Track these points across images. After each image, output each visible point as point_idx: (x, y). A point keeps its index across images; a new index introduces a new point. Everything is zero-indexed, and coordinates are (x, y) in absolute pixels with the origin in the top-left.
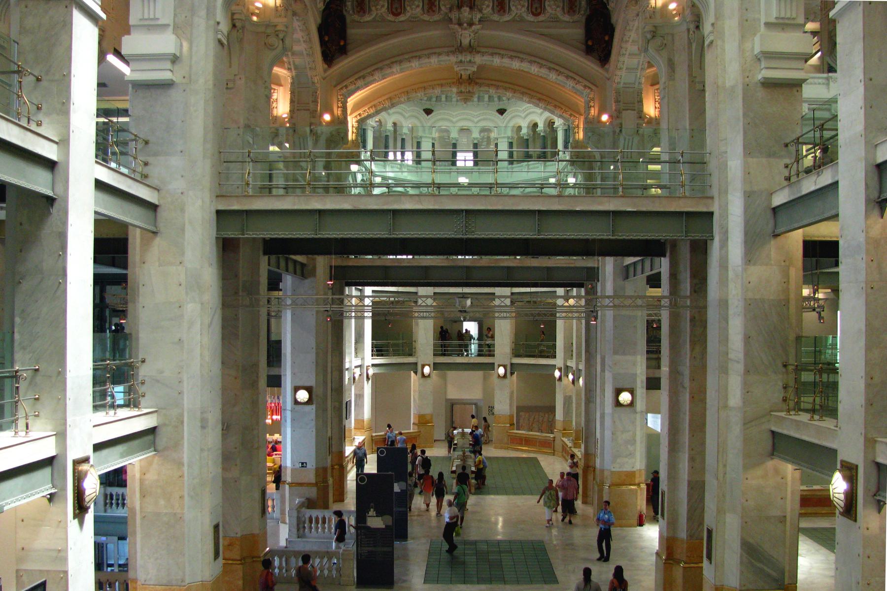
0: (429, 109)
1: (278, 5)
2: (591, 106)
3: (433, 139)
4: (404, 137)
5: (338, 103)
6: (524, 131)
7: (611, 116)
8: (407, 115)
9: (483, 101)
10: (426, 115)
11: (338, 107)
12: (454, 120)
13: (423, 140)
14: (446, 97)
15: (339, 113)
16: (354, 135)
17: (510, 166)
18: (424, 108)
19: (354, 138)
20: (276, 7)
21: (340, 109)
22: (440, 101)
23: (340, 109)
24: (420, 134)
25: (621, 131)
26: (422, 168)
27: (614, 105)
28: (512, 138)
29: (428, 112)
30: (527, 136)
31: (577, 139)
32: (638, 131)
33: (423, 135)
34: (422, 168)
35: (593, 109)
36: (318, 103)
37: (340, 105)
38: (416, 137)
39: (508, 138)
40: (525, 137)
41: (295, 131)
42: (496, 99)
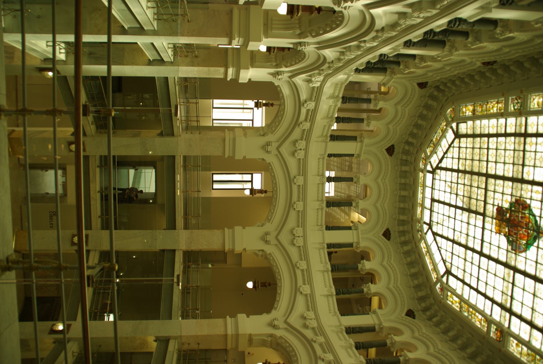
0: (393, 151)
3: (359, 156)
4: (365, 122)
6: (367, 265)
8: (391, 126)
9: (399, 213)
10: (386, 147)
12: (379, 180)
13: (359, 144)
14: (406, 172)
17: (326, 246)
18: (395, 147)
22: (401, 165)
24: (366, 141)
26: (326, 142)
28: (357, 248)
29: (390, 150)
30: (362, 269)
33: (364, 144)
34: (326, 142)
38: (361, 136)
39: (358, 243)
40: (360, 266)
42: (401, 228)
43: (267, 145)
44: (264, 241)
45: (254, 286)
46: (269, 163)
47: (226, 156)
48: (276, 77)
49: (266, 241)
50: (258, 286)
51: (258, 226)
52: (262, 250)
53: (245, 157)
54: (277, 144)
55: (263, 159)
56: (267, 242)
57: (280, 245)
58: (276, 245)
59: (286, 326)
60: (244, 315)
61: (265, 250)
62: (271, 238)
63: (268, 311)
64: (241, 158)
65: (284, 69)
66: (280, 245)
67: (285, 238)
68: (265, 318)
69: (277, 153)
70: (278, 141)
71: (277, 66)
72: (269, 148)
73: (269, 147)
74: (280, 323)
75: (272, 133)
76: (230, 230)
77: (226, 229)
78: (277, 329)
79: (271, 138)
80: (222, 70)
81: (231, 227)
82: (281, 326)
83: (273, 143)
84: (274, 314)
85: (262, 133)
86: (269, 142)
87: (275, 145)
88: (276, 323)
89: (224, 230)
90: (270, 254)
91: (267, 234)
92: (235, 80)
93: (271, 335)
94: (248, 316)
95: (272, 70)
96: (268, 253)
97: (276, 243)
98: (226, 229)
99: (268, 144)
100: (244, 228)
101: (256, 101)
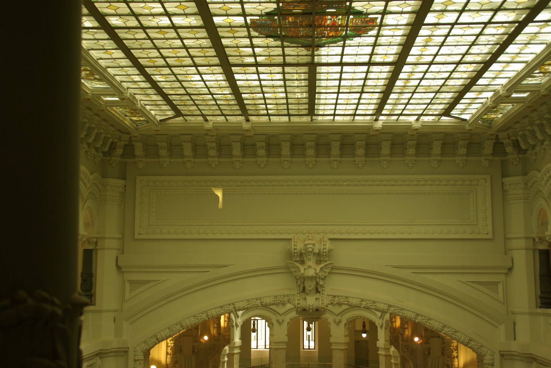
1: (168, 363)
2: (405, 328)
5: (214, 325)
7: (420, 337)
11: (214, 328)
15: (215, 332)
16: (226, 323)
19: (226, 325)
20: (167, 364)
21: (215, 329)
23: (215, 329)
25: (429, 353)
27: (423, 332)
31: (394, 327)
32: (442, 353)
35: (407, 330)
36: (199, 329)
37: (215, 326)
41: (181, 351)
43: (279, 321)
44: (339, 324)
45: (365, 333)
46: (290, 319)
47: (286, 347)
48: (238, 326)
49: (339, 322)
50: (364, 330)
51: (330, 326)
52: (345, 325)
53: (286, 335)
54: (278, 316)
55: (288, 323)
56: (340, 322)
57: (342, 313)
58: (341, 316)
59: (381, 319)
60: (378, 342)
61: (344, 323)
62: (338, 319)
63: (377, 327)
64: (287, 338)
65: (234, 323)
66: (342, 313)
67: (337, 310)
68: (379, 329)
69: (283, 315)
70: (276, 315)
71: (233, 326)
72: (281, 320)
73: (279, 321)
74: (381, 321)
75: (271, 320)
76: (333, 345)
77: (332, 347)
78: (383, 325)
79: (274, 321)
80: (235, 356)
81: (331, 344)
82: (381, 322)
83: (278, 318)
84: (377, 324)
85: (271, 325)
86: (277, 321)
87: (278, 317)
88: (380, 324)
89: (332, 349)
90: (347, 320)
91: (335, 321)
92: (240, 347)
93: (386, 328)
94: (378, 340)
95: (235, 328)
96: (346, 321)
97: (340, 316)
98: (332, 347)
99: (278, 321)
100: (331, 336)
101: (252, 331)
